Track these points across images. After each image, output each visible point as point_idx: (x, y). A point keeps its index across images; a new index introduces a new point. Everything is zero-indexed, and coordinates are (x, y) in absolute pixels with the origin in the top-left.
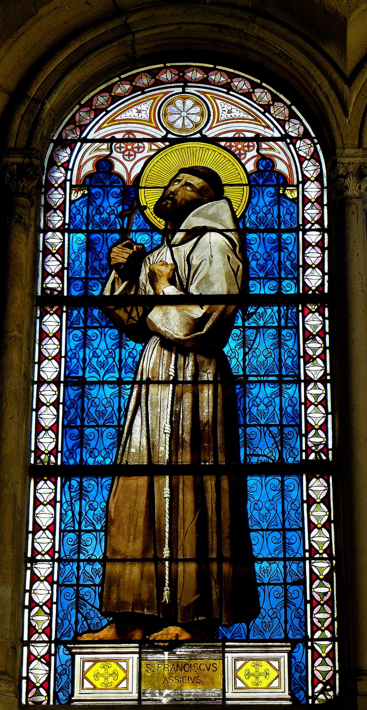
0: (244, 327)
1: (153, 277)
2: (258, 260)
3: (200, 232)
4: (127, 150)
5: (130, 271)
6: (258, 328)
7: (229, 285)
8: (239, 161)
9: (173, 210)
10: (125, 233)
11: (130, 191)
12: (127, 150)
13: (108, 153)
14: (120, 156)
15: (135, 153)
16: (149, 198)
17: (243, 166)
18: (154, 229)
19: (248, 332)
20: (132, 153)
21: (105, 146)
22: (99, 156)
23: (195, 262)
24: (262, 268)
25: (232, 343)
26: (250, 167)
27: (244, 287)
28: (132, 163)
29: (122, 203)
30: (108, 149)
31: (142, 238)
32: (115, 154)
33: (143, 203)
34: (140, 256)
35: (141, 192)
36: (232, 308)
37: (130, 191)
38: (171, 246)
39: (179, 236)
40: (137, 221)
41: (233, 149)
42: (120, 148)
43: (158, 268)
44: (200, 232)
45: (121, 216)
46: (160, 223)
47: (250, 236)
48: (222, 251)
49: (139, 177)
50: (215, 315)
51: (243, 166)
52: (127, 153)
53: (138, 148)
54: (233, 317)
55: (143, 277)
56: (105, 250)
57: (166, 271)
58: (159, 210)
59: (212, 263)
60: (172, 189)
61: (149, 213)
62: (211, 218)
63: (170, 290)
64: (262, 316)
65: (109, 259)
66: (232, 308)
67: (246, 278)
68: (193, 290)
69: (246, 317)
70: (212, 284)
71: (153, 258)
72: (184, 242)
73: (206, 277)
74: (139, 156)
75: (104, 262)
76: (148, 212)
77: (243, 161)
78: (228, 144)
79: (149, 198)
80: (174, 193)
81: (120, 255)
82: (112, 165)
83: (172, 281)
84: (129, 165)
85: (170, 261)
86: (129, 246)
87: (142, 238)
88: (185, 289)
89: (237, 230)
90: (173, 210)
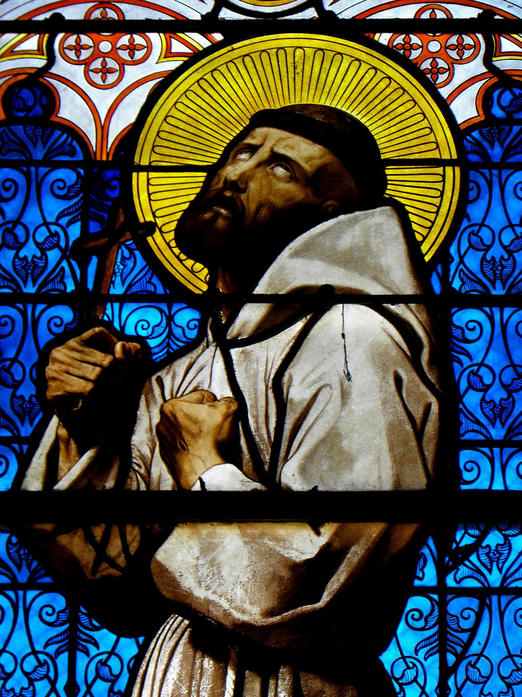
0: (441, 587)
1: (172, 438)
2: (486, 388)
3: (314, 302)
4: (97, 54)
5: (102, 418)
6: (483, 594)
7: (399, 462)
8: (432, 90)
9: (235, 235)
10: (89, 304)
11: (106, 178)
12: (97, 54)
13: (40, 62)
14: (76, 74)
15: (122, 64)
16: (162, 199)
17: (444, 106)
18: (176, 293)
19: (455, 606)
20: (111, 63)
21: (32, 43)
22: (14, 73)
23: (298, 393)
24: (498, 412)
25: (407, 638)
26: (465, 109)
27: (444, 469)
28: (113, 95)
29: (83, 214)
30: (40, 51)
31: (140, 320)
32: (61, 67)
33: (145, 215)
34: (133, 373)
35: (139, 179)
36: (406, 532)
37: (106, 178)
38: (225, 346)
39: (251, 315)
40: (127, 270)
41: (415, 54)
42: (78, 48)
43: (186, 409)
44: (314, 302)
45: (78, 253)
46: (195, 276)
47: (464, 317)
48: (379, 358)
49: (132, 135)
50: (356, 553)
51: (444, 106)
52: (97, 64)
53: (132, 48)
54: (411, 559)
55: (142, 439)
56: (30, 356)
57: (211, 418)
58: (192, 233)
59: (348, 394)
60: (232, 172)
61: (163, 244)
62: (349, 260)
63: (223, 477)
64: (496, 557)
65: (41, 382)
66: (406, 532)
67: (450, 442)
68: (291, 476)
69: (450, 559)
70: (346, 460)
71: (172, 378)
72: (263, 332)
73: (332, 439)
74: (133, 74)
75: (27, 390)
76: (157, 241)
77: (445, 92)
78: (400, 39)
79: (162, 199)
80: (238, 186)
81: (74, 369)
82: (52, 101)
83: (227, 451)
84: (103, 100)
85: (222, 389)
86: (102, 343)
87: (140, 320)
88: (266, 472)
89: (423, 298)
90: (235, 235)
